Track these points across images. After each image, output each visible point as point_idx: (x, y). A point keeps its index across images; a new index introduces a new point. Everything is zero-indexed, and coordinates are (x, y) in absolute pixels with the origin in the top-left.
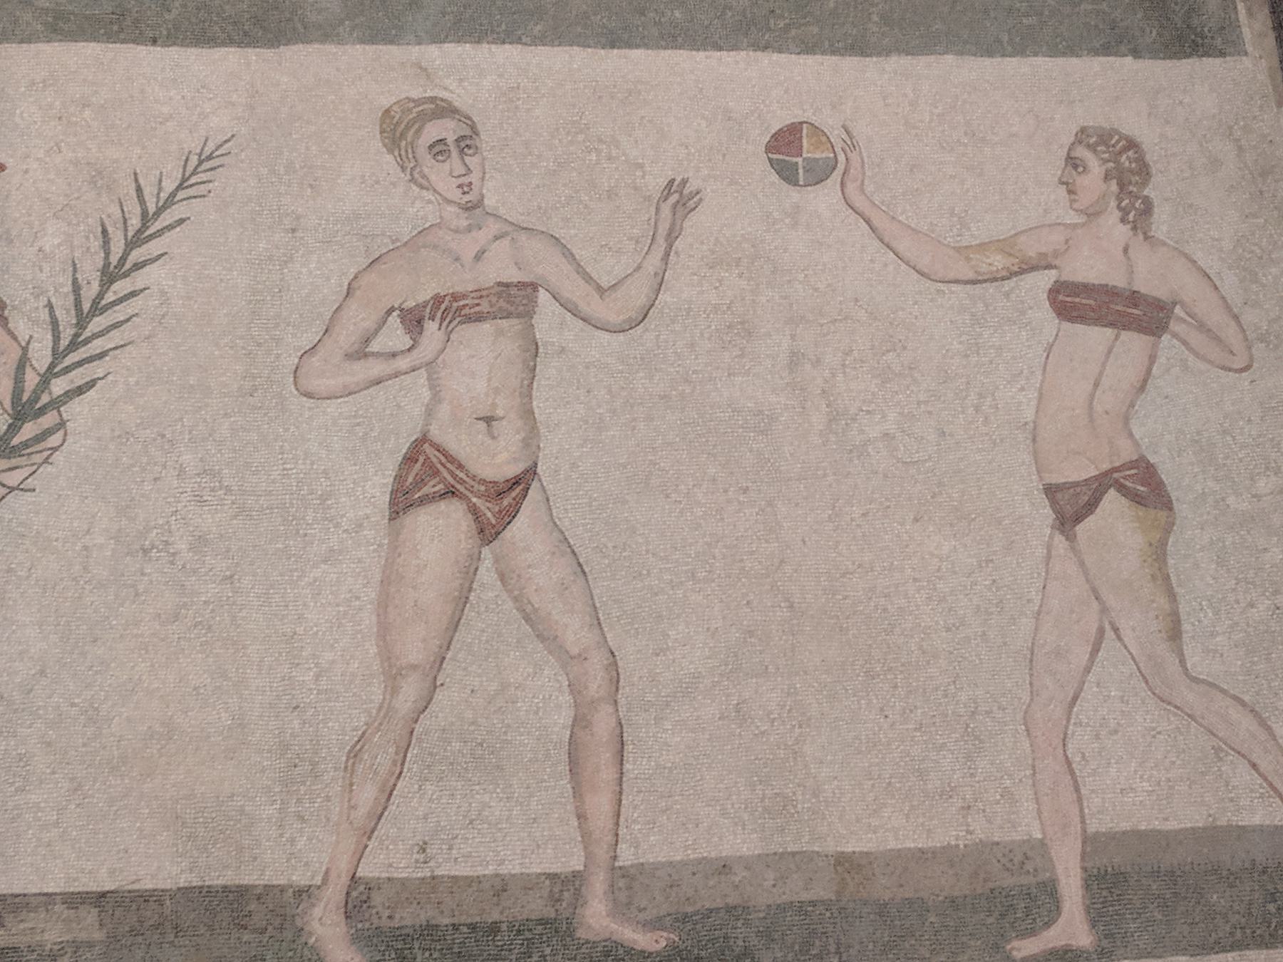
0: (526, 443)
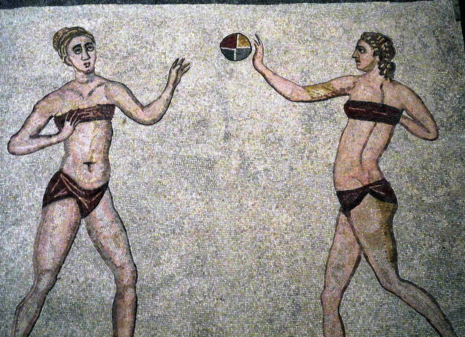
0: (104, 174)
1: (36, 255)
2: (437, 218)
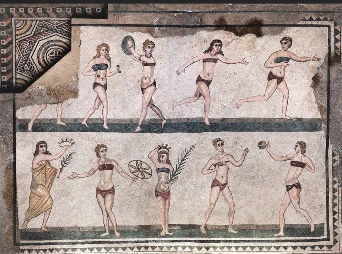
1: (210, 199)
2: (311, 193)
